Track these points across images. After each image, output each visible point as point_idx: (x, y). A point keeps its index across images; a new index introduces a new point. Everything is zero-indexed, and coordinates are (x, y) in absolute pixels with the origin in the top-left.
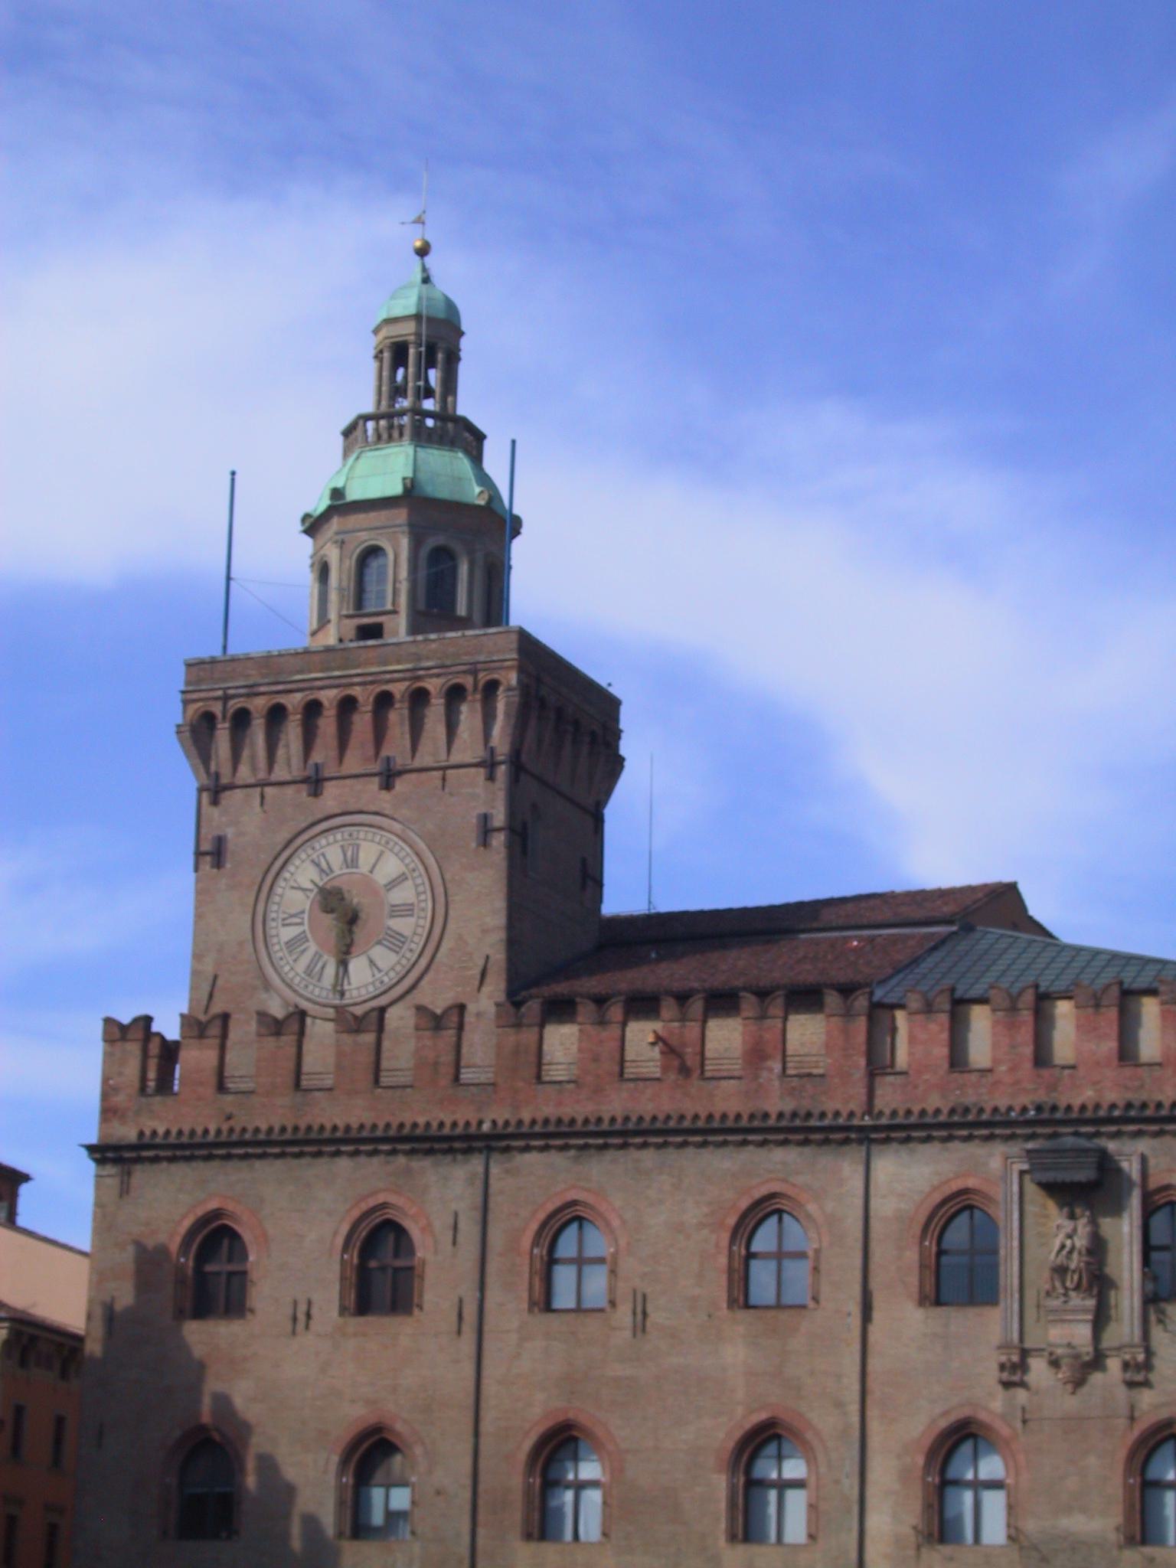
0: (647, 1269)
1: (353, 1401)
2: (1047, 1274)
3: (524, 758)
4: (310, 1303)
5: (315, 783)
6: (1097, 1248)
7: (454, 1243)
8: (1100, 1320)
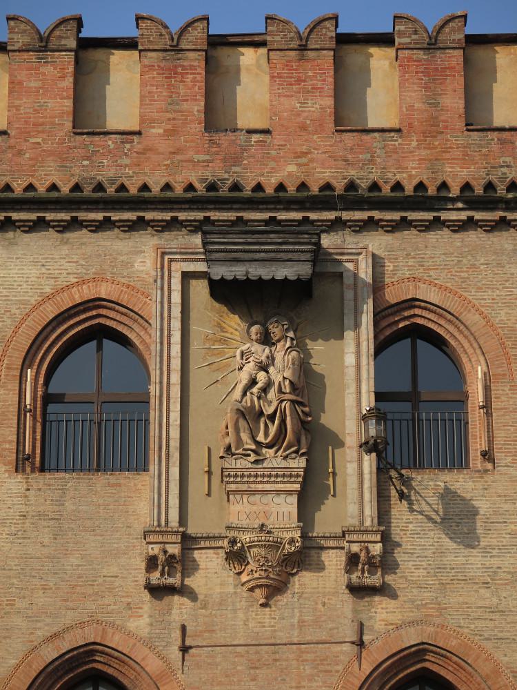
2: (229, 417)
6: (307, 387)
8: (311, 492)
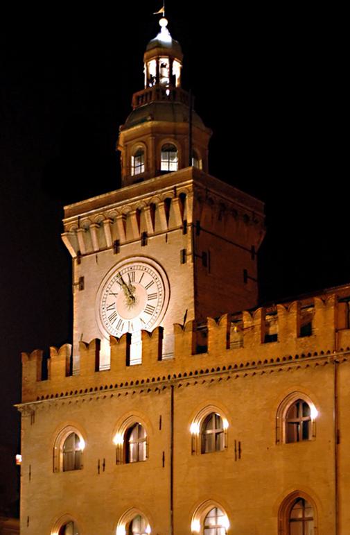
0: (241, 431)
1: (123, 499)
3: (201, 225)
4: (104, 460)
5: (117, 245)
7: (160, 429)
